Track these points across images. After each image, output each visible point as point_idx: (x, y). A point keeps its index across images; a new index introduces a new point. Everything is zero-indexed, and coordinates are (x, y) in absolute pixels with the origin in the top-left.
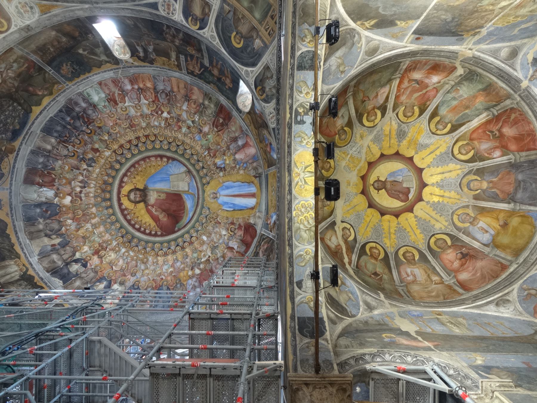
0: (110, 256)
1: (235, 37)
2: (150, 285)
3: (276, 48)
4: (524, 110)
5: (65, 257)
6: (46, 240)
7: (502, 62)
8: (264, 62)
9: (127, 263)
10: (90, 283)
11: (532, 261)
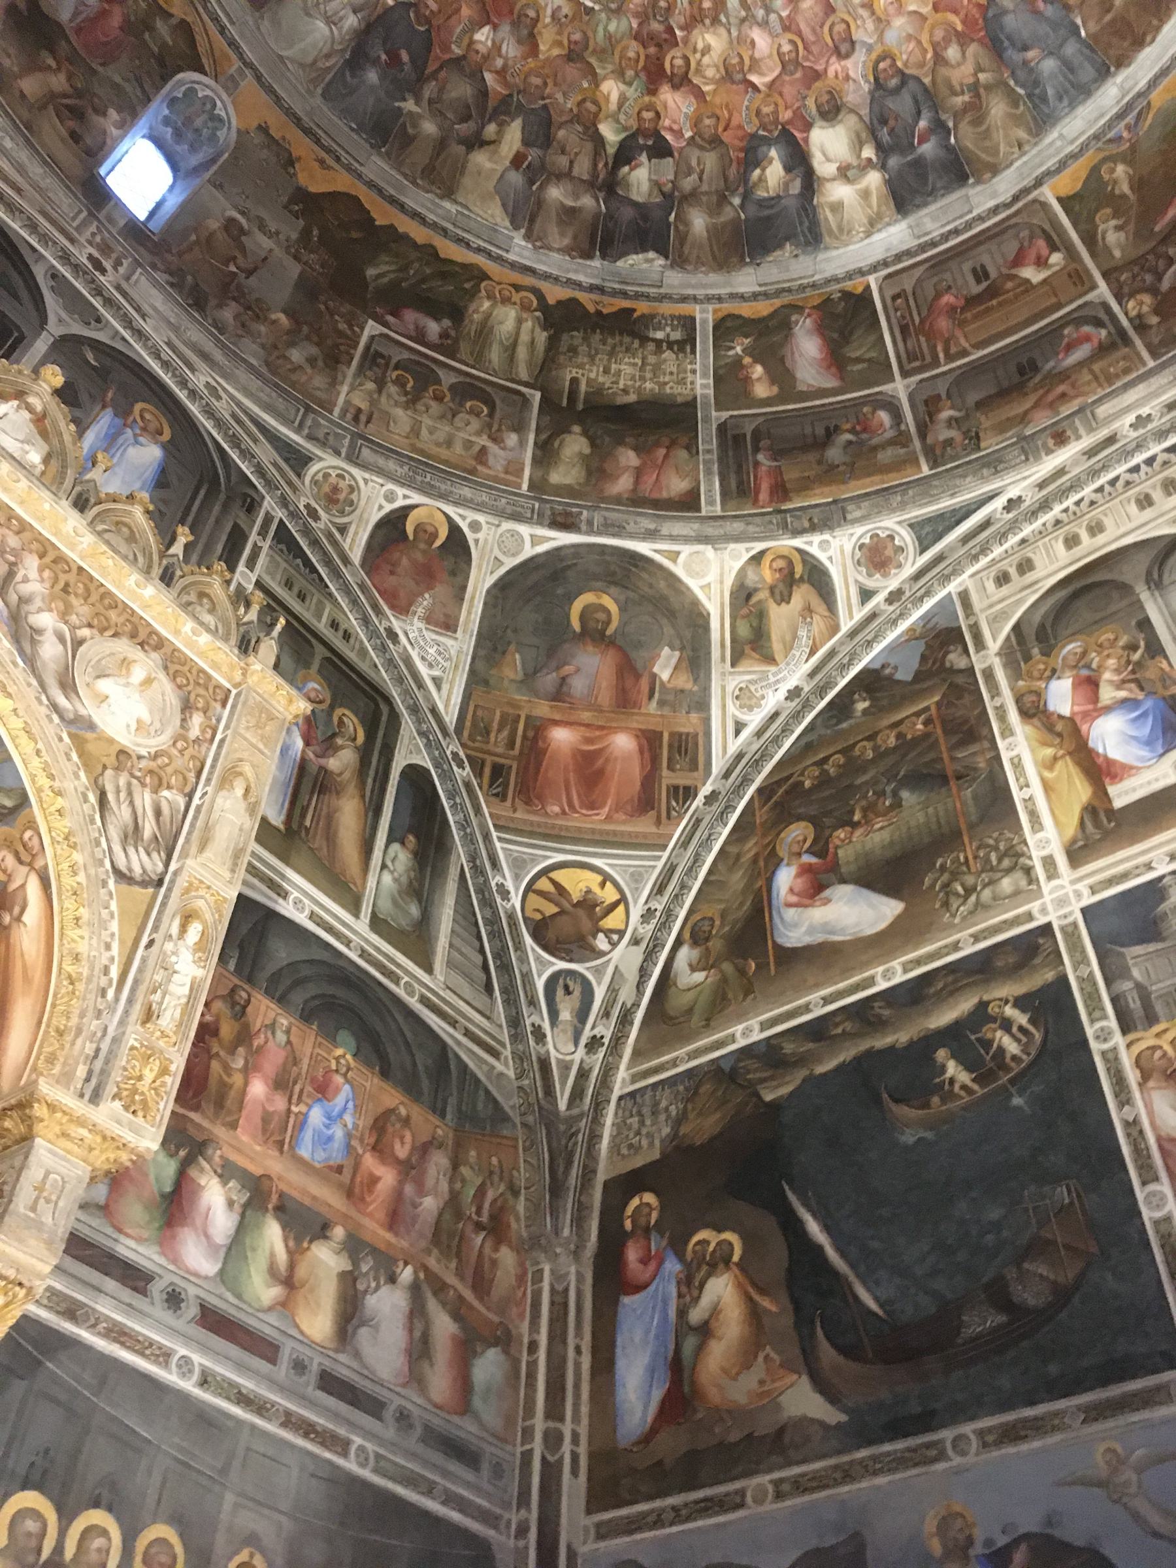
0: (707, 50)
2: (939, 34)
5: (582, 168)
6: (480, 159)
9: (786, 29)
10: (734, 192)
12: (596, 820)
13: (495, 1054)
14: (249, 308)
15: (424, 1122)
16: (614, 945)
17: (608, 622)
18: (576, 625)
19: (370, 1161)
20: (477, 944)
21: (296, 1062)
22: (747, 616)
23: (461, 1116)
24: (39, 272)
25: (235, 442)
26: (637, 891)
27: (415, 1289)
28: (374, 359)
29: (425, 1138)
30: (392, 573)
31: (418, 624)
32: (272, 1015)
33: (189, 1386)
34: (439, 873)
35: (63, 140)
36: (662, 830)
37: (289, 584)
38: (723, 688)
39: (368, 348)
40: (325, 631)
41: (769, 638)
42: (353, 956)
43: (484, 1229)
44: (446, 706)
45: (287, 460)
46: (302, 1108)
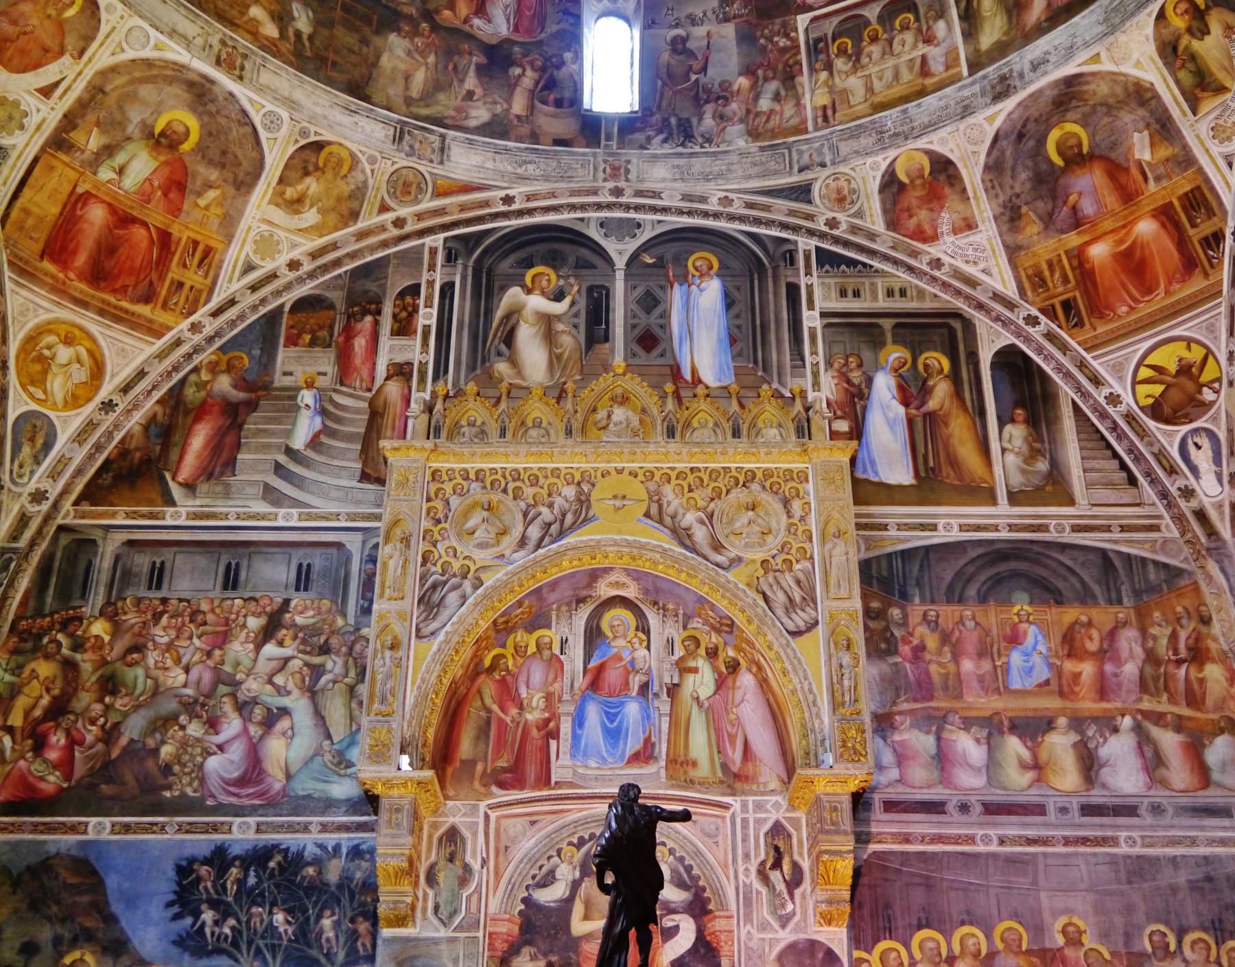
12: (1159, 300)
13: (1156, 528)
14: (719, 98)
15: (1103, 616)
16: (1217, 392)
17: (1080, 145)
18: (1058, 161)
19: (1069, 666)
20: (1109, 453)
21: (988, 633)
22: (1183, 66)
23: (1137, 593)
24: (594, 233)
25: (758, 221)
26: (1216, 339)
27: (1138, 729)
28: (817, 47)
29: (1108, 627)
30: (911, 216)
31: (949, 239)
32: (957, 614)
33: (994, 848)
34: (1053, 421)
35: (554, 116)
36: (1212, 280)
37: (843, 293)
38: (1198, 136)
39: (807, 42)
40: (886, 305)
41: (1211, 74)
42: (1004, 535)
43: (1184, 661)
44: (1004, 283)
45: (796, 200)
46: (1004, 659)
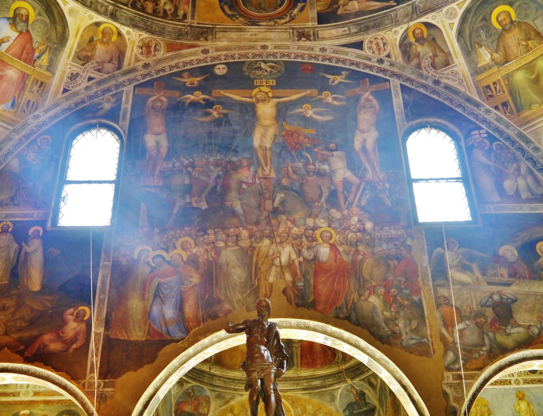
1: (509, 14)
3: (468, 93)
4: (332, 366)
7: (367, 377)
8: (457, 57)
11: (214, 383)
